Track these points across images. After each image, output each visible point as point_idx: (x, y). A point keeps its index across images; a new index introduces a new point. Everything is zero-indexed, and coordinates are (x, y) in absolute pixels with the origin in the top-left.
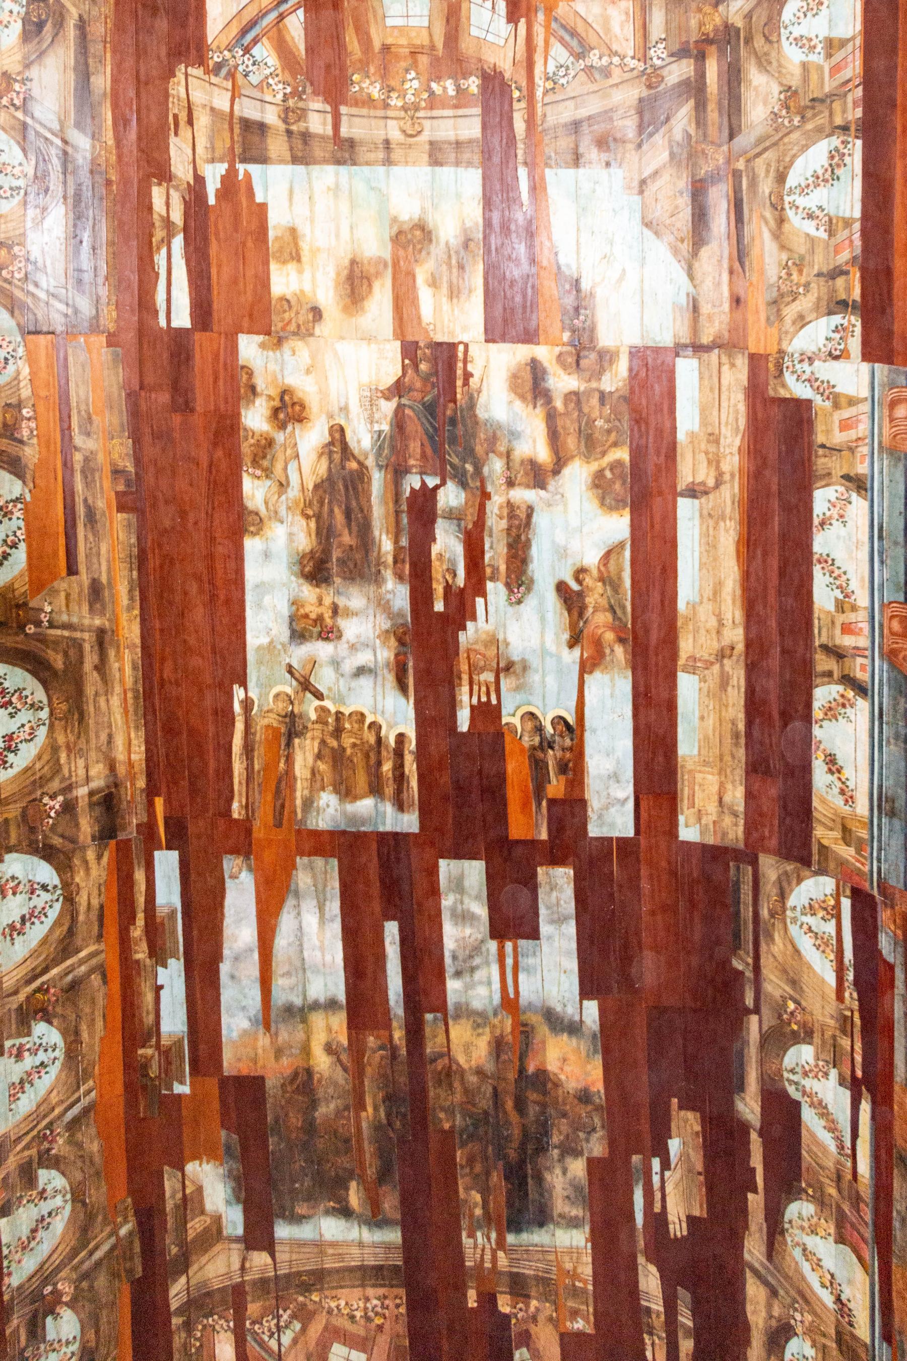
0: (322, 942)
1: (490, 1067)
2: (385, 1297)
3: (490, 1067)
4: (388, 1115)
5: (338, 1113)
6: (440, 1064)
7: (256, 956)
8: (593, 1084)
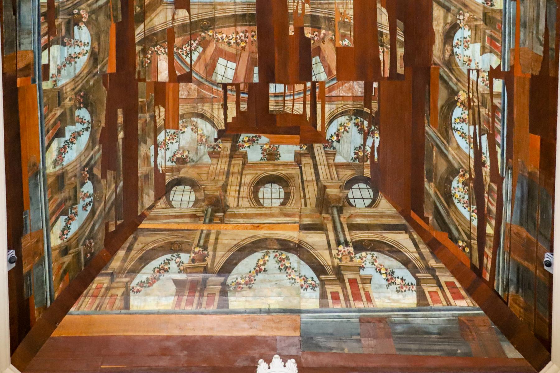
2: (247, 32)
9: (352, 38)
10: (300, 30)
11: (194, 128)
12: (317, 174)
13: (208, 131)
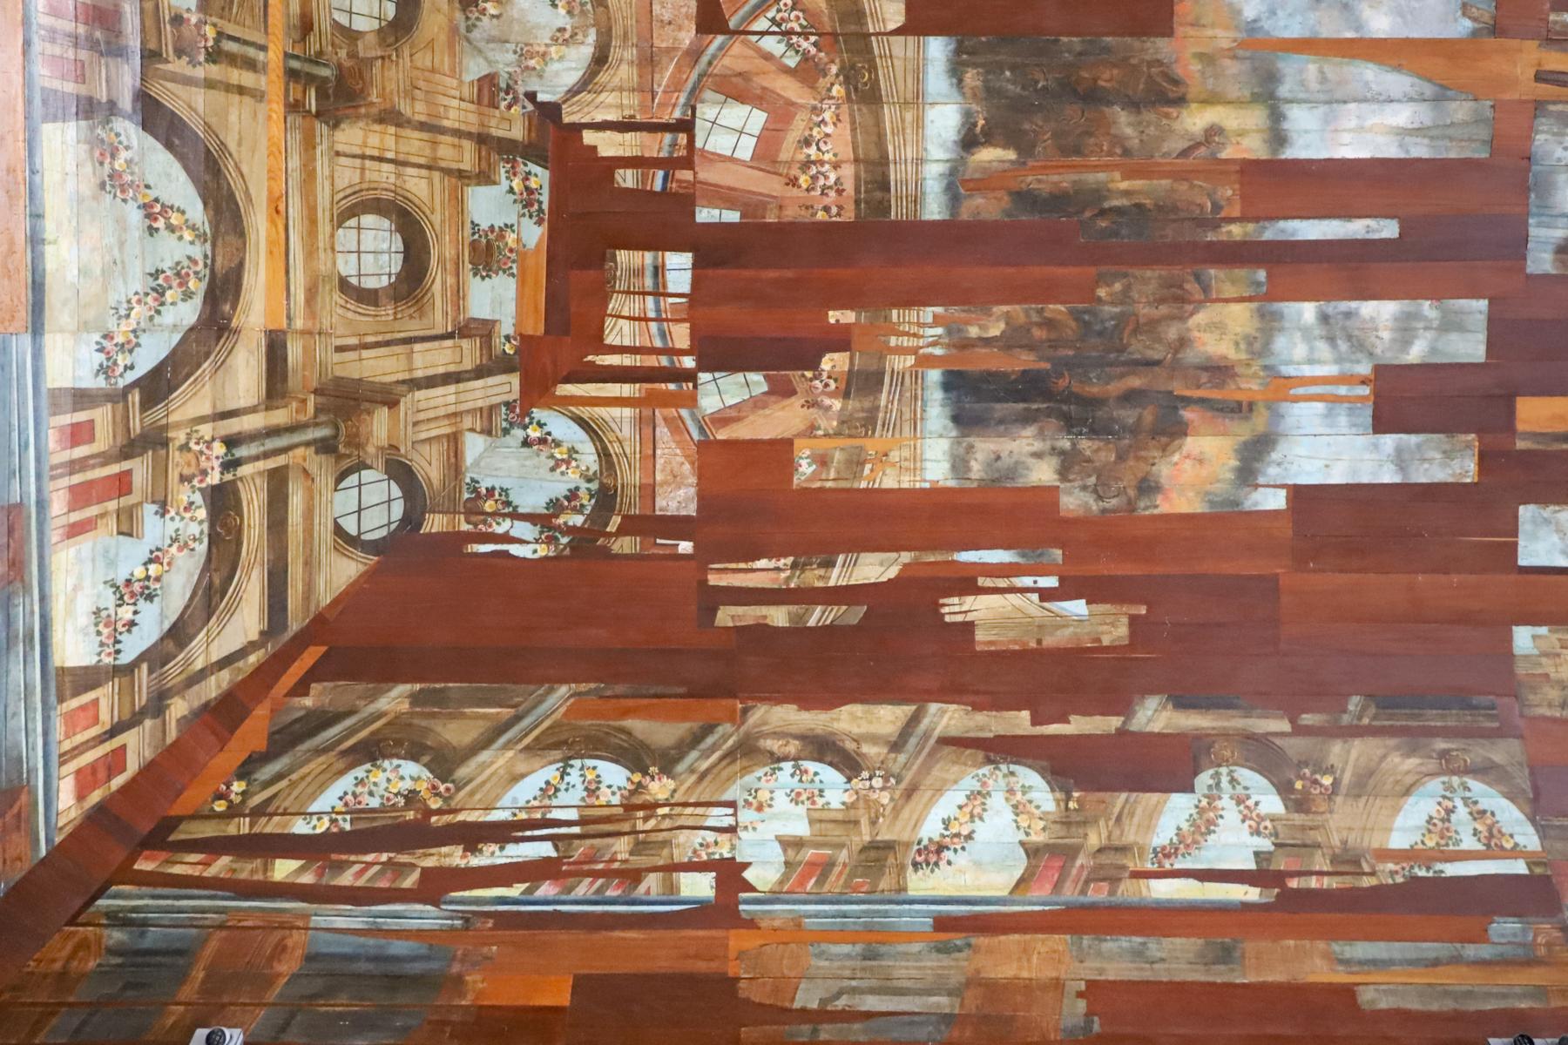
0: (1370, 130)
1: (1190, 356)
2: (840, 192)
3: (1190, 356)
4: (1119, 211)
5: (1118, 140)
6: (1191, 286)
7: (1349, 35)
8: (1167, 499)
9: (817, 485)
10: (840, 340)
11: (567, 35)
12: (431, 382)
13: (557, 74)
